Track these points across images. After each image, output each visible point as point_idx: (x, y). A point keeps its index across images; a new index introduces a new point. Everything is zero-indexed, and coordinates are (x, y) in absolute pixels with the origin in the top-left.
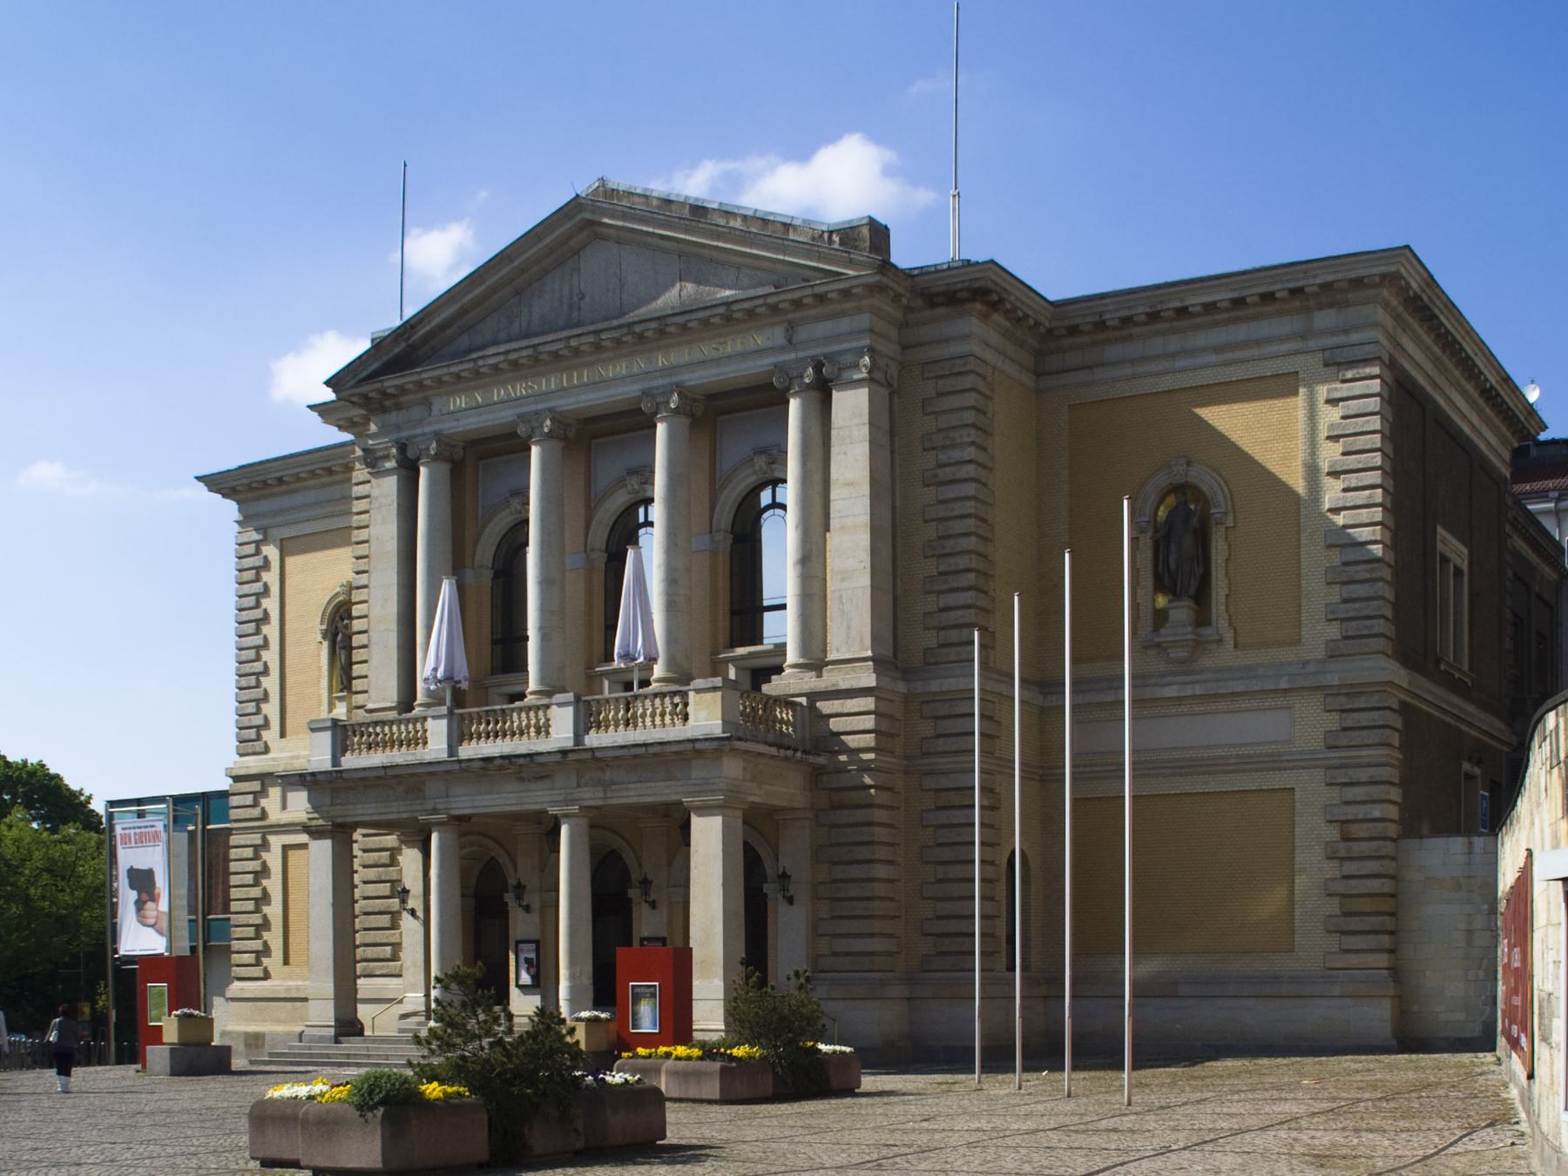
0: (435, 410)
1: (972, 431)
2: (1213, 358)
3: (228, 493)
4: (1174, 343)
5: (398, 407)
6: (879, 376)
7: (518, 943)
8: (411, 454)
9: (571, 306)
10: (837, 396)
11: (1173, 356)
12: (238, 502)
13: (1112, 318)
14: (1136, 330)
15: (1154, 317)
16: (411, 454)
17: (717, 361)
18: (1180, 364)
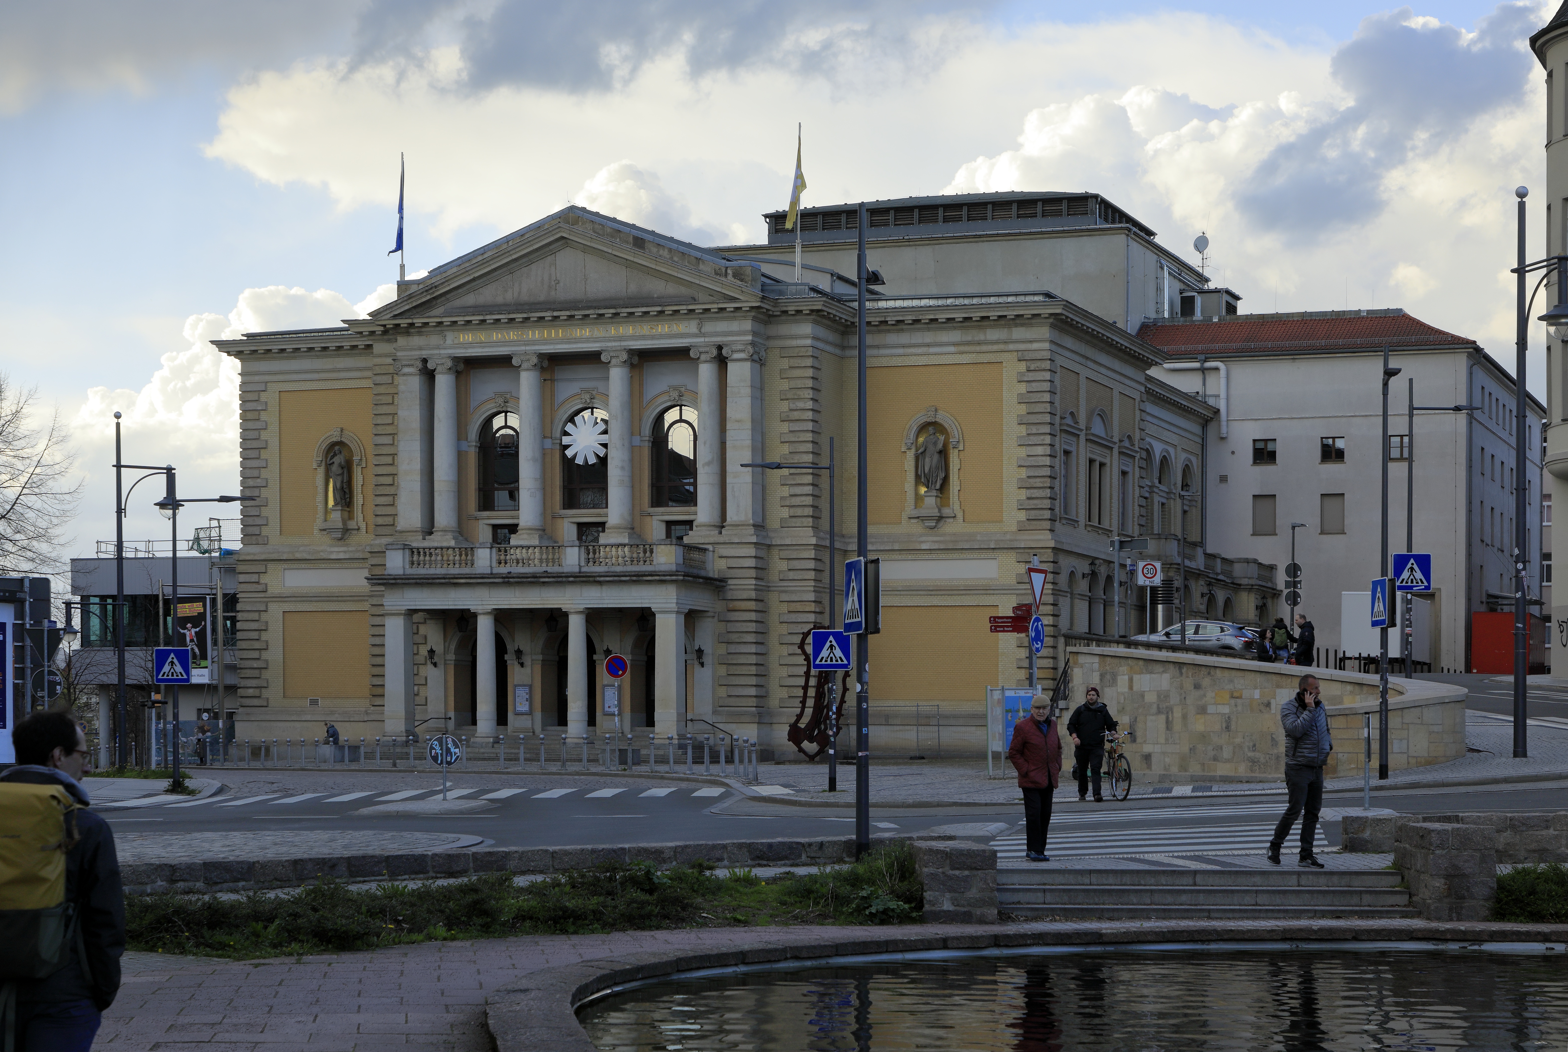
0: (449, 341)
1: (811, 392)
2: (952, 349)
3: (238, 354)
4: (929, 337)
5: (420, 333)
6: (756, 357)
7: (516, 686)
8: (430, 366)
9: (550, 287)
10: (731, 366)
11: (928, 345)
12: (241, 360)
13: (891, 319)
14: (905, 327)
15: (917, 321)
16: (430, 366)
17: (653, 337)
18: (932, 350)
